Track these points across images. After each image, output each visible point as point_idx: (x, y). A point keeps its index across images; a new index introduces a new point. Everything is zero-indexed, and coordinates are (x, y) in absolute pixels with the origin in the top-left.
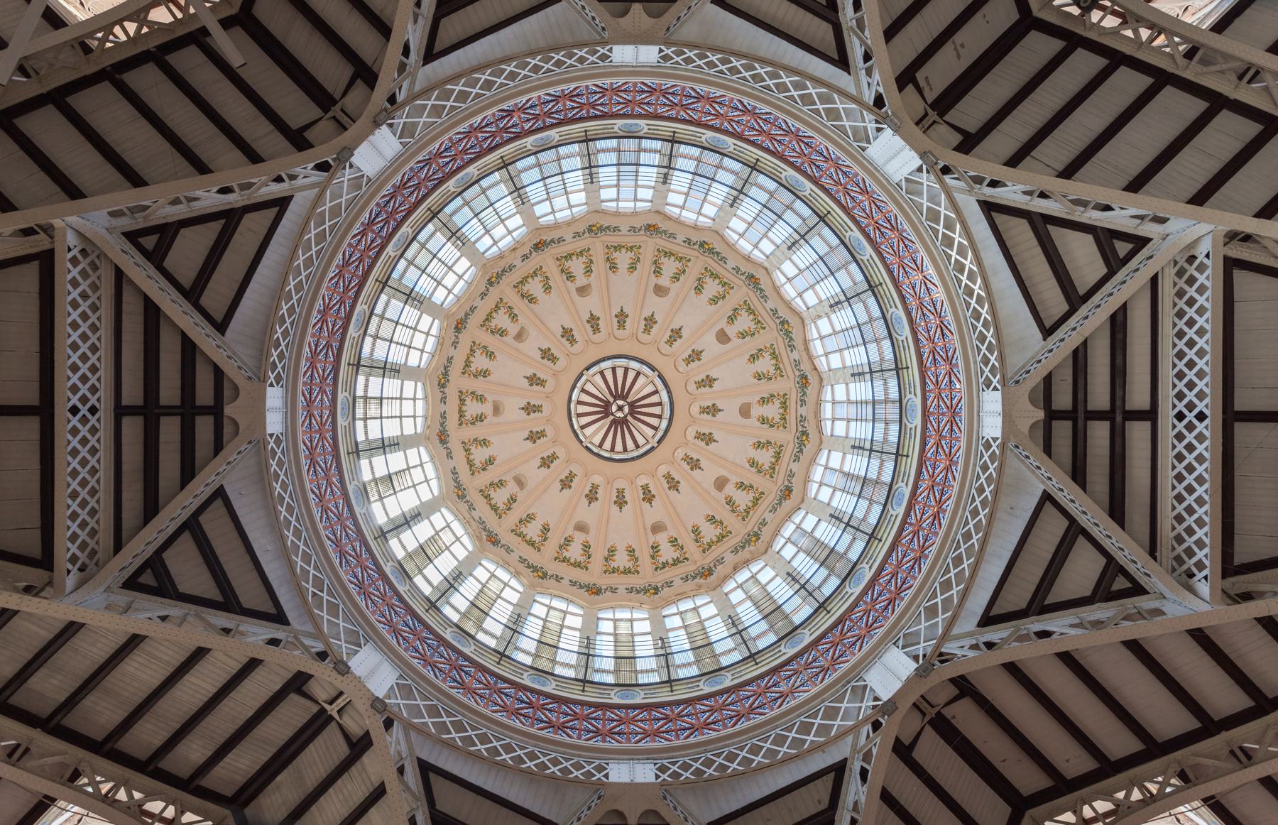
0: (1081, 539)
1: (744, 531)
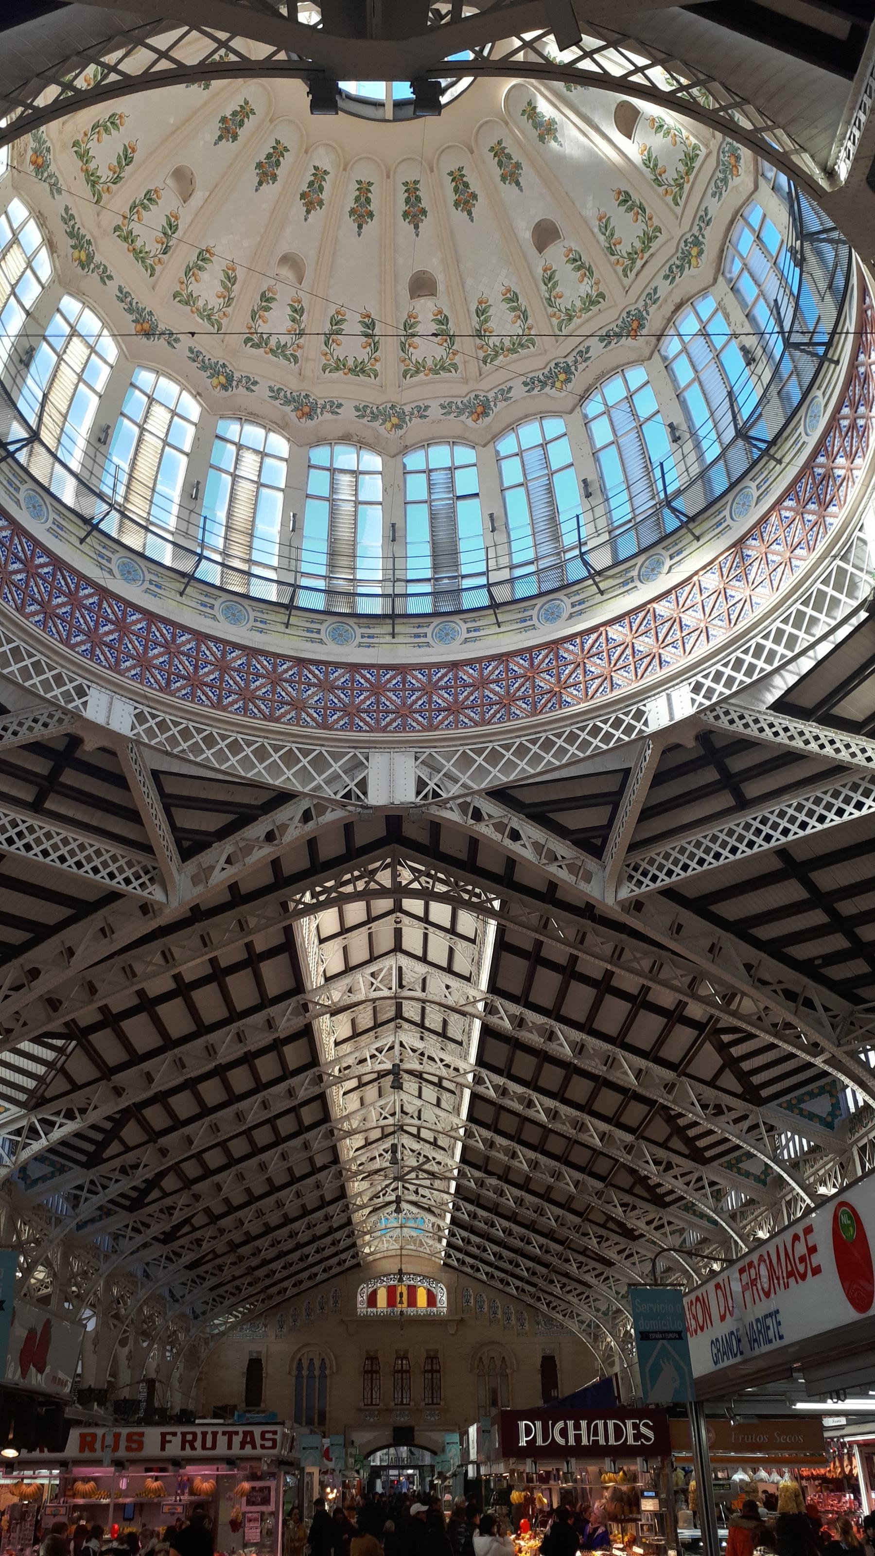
0: (609, 808)
1: (393, 395)
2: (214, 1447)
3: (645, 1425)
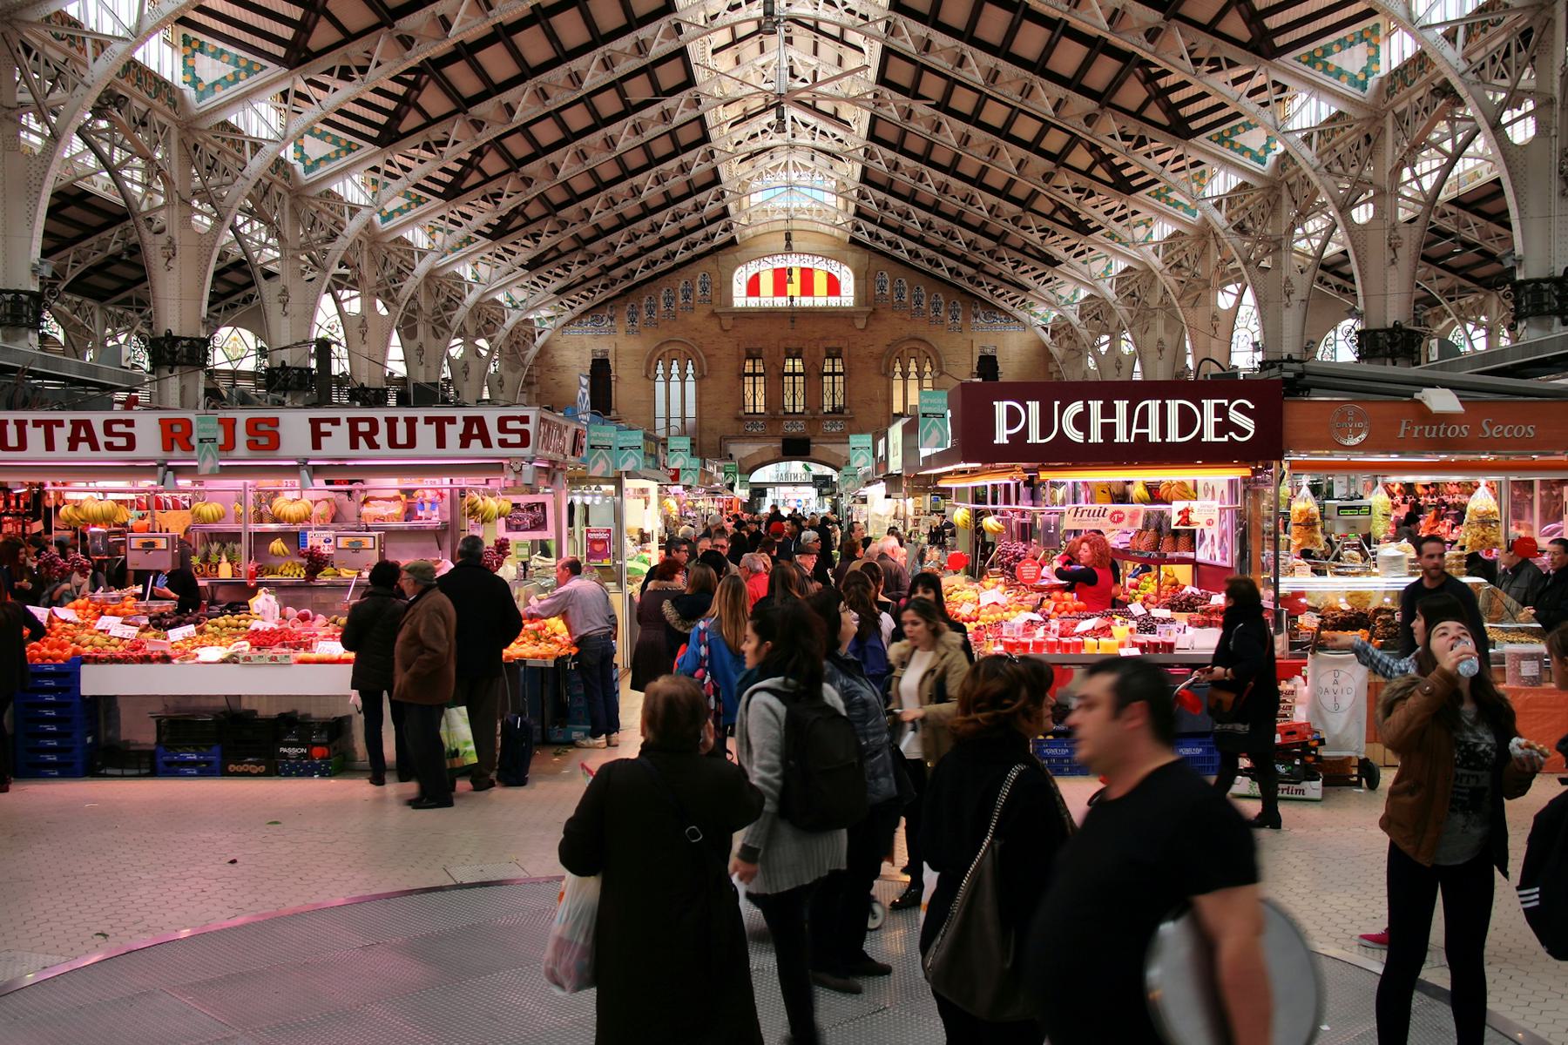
2: (411, 443)
3: (1240, 408)
